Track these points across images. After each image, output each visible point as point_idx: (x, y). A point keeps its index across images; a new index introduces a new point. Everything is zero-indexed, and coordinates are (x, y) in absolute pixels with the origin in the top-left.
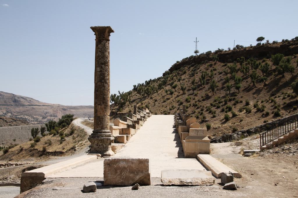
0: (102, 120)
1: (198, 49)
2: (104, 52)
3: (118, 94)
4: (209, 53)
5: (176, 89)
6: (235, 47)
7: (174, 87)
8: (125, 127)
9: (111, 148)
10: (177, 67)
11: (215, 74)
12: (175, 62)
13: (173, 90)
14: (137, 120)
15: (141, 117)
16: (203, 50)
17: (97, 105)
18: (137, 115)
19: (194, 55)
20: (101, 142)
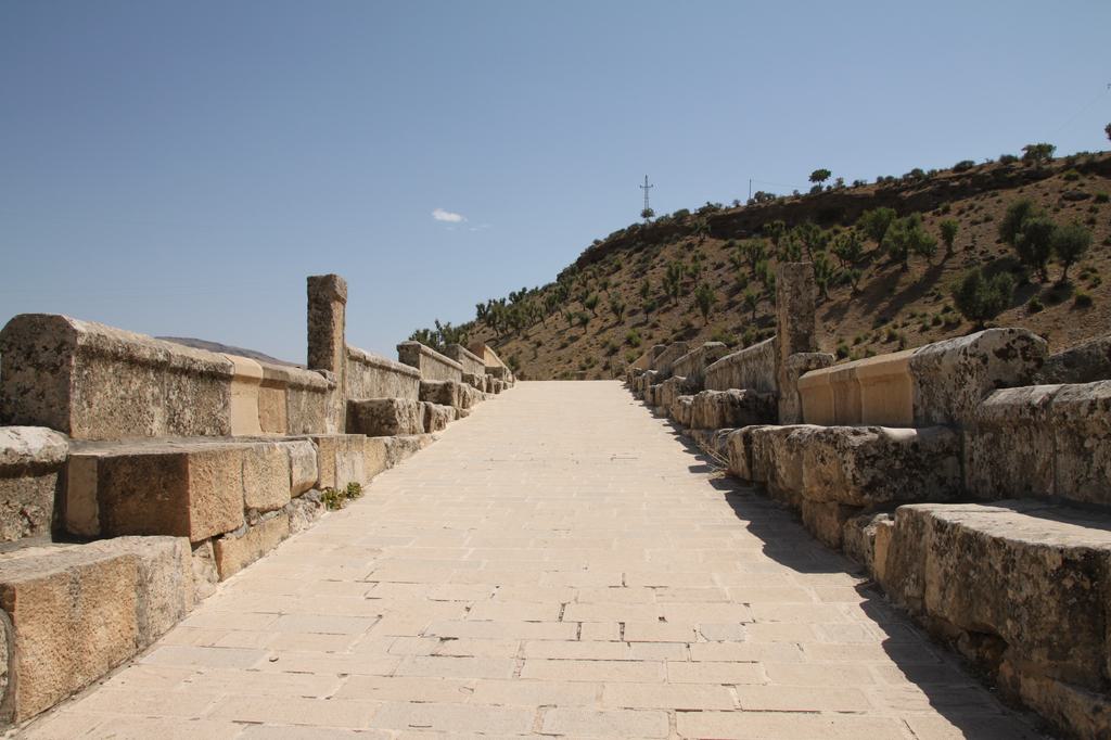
1: (653, 206)
3: (434, 329)
4: (682, 215)
5: (597, 310)
6: (753, 197)
7: (592, 306)
10: (595, 256)
11: (705, 269)
12: (591, 244)
13: (589, 313)
16: (665, 208)
19: (642, 221)
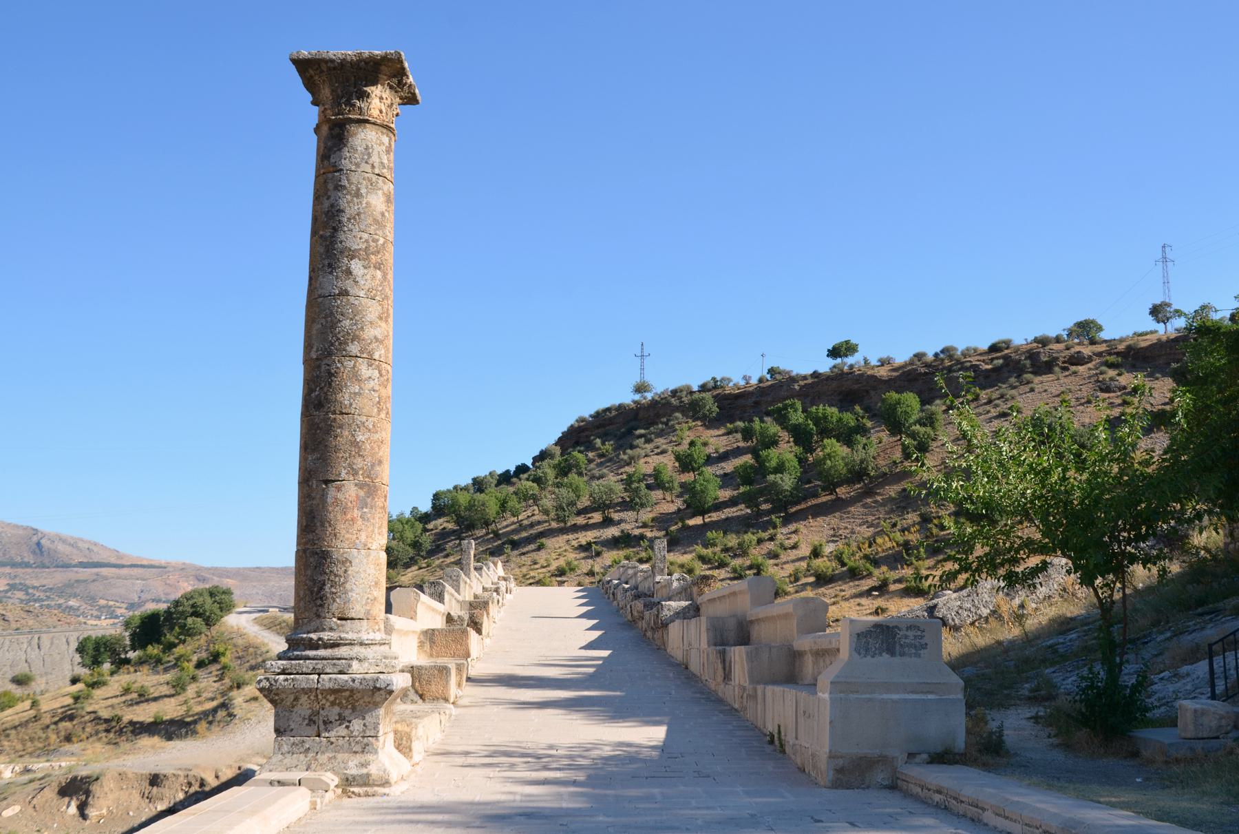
0: (346, 571)
1: (650, 378)
2: (363, 191)
8: (439, 623)
9: (391, 736)
14: (472, 599)
15: (484, 589)
16: (662, 383)
17: (314, 483)
18: (475, 581)
20: (333, 704)
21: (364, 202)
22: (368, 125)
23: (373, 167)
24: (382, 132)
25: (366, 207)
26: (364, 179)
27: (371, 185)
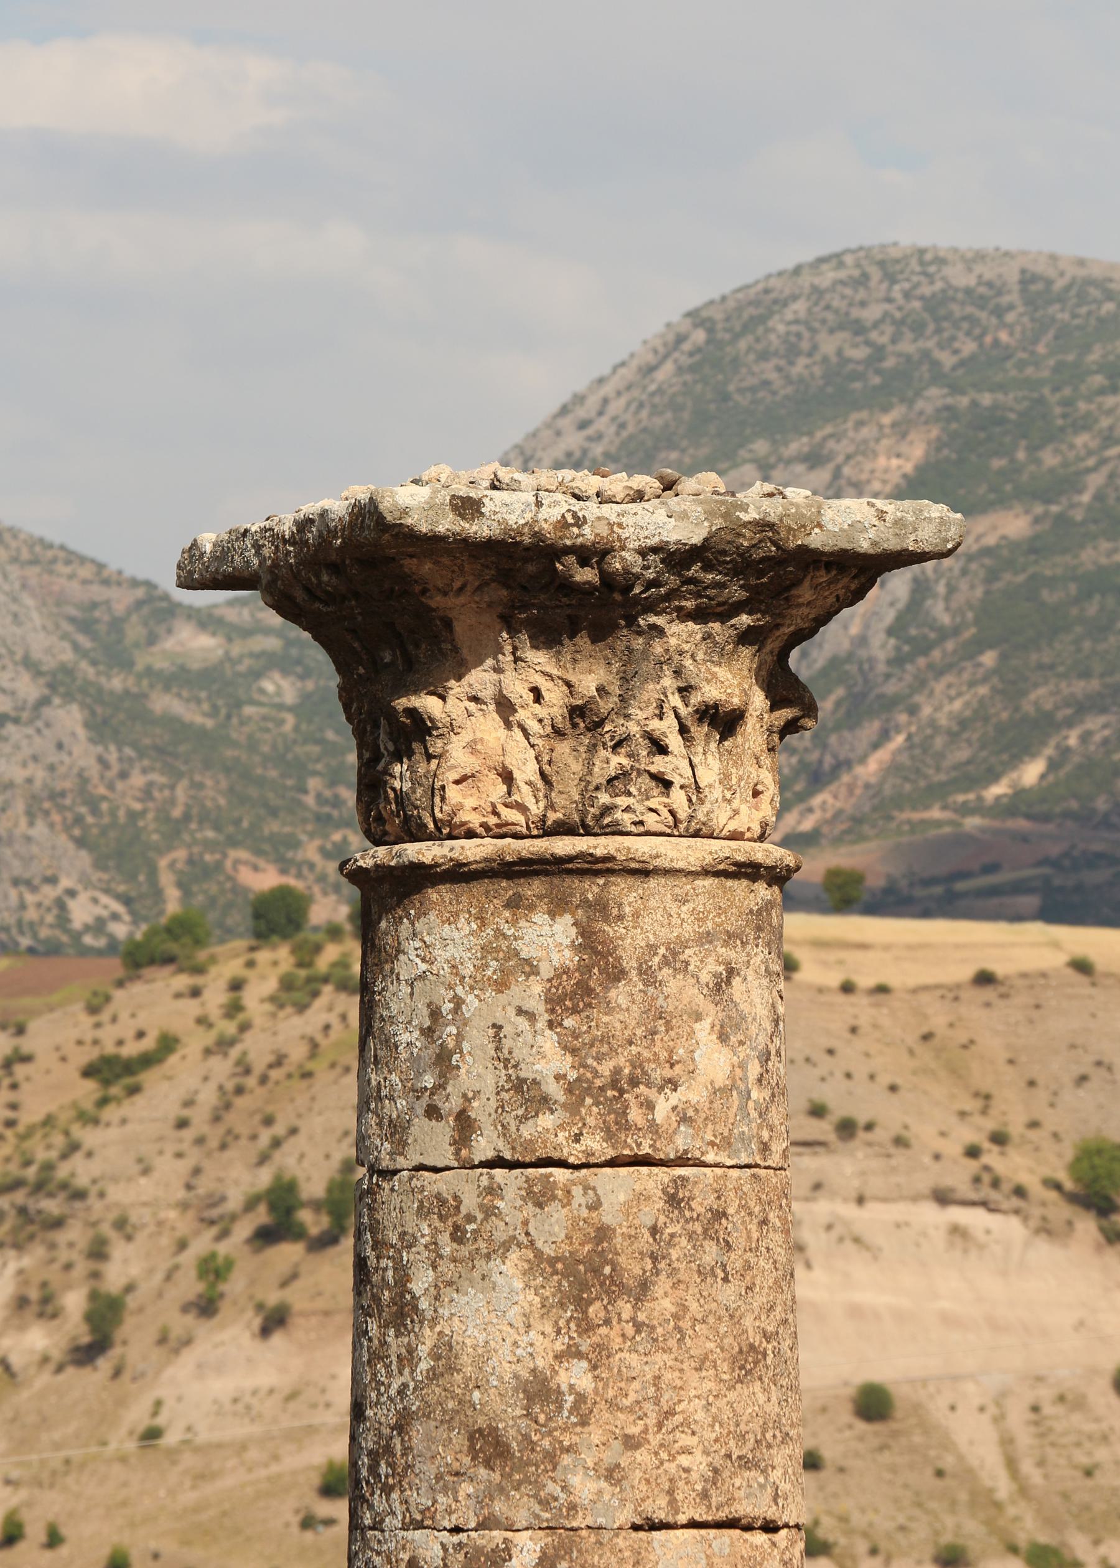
2: (421, 1282)
21: (423, 1350)
22: (433, 894)
23: (465, 1125)
24: (514, 904)
25: (433, 1375)
26: (422, 1212)
27: (458, 1235)
